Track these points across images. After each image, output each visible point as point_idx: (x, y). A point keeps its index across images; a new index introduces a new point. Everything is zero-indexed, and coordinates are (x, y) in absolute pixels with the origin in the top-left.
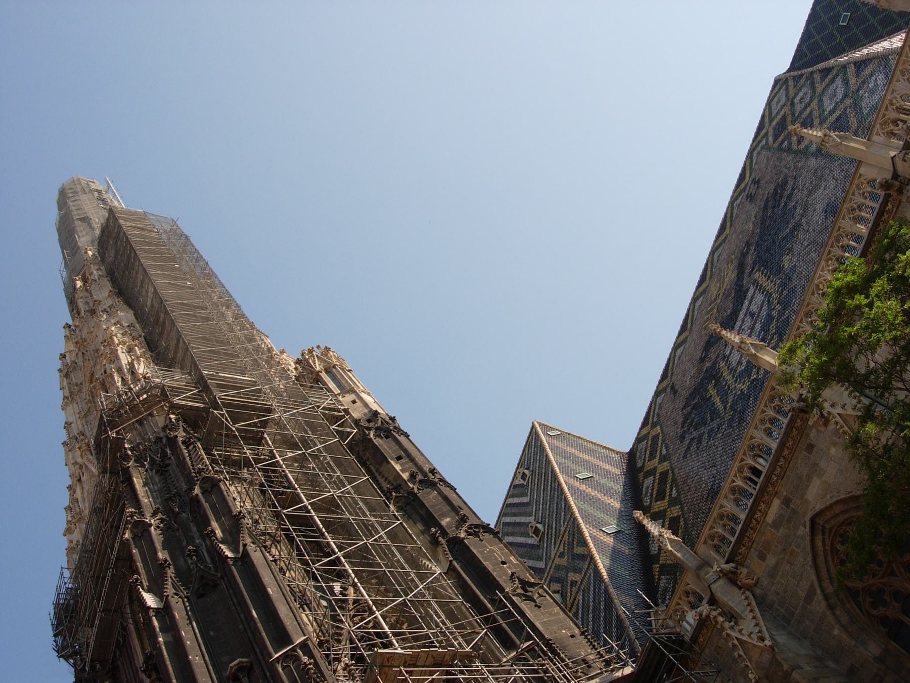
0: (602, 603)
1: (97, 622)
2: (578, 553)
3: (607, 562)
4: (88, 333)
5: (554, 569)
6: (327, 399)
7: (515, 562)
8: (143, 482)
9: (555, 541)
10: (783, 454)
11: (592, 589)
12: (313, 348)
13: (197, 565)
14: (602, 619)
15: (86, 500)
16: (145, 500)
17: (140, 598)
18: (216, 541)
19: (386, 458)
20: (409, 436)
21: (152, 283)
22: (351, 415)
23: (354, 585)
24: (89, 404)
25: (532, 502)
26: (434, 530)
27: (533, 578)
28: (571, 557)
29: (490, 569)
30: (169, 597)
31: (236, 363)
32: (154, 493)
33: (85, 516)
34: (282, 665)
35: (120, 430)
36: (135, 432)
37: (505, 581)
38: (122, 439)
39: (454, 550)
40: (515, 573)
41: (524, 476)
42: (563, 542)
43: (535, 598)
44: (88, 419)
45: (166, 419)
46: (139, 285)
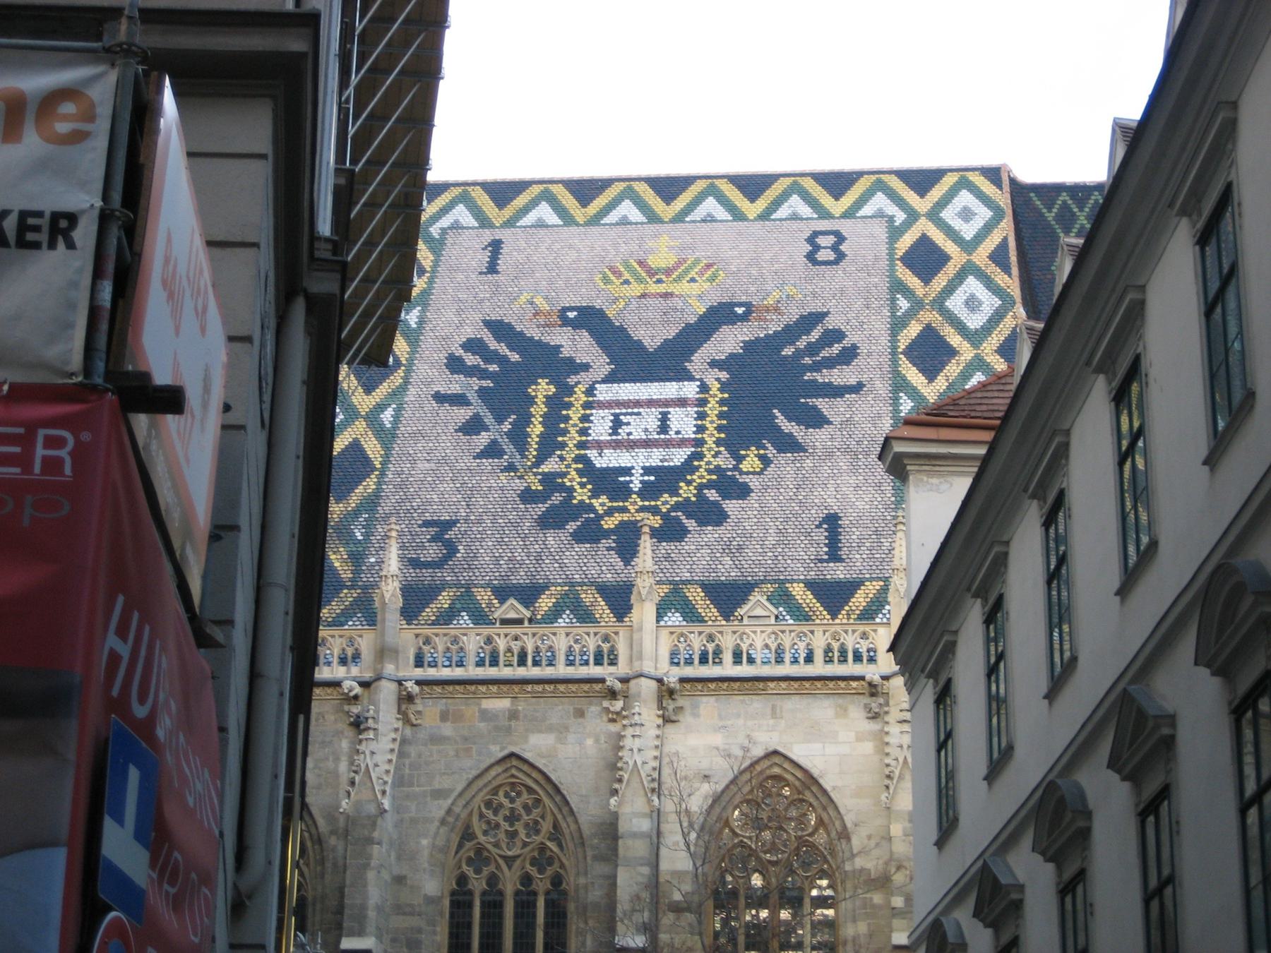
10: (558, 686)
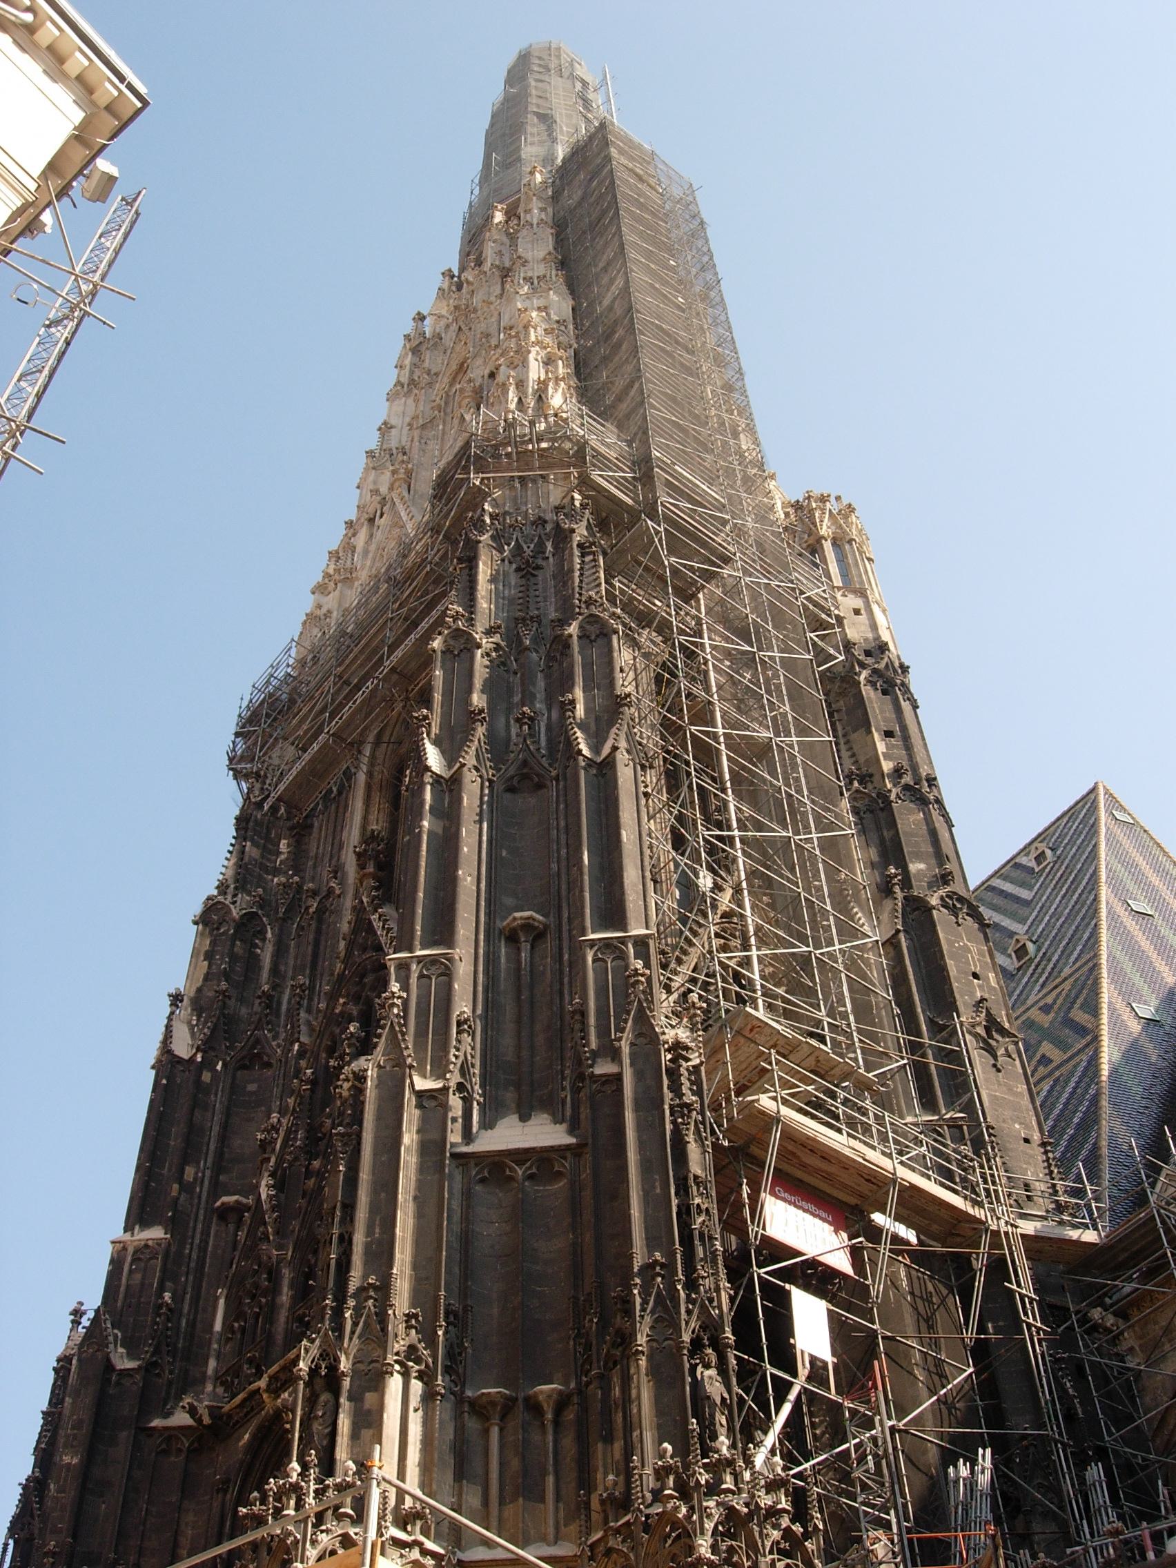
0: (1079, 1115)
1: (316, 747)
2: (1077, 1019)
3: (1117, 1056)
4: (484, 301)
5: (1023, 1023)
6: (819, 587)
7: (993, 983)
8: (491, 575)
9: (1044, 983)
11: (1072, 1084)
12: (829, 496)
13: (525, 740)
14: (1066, 1137)
15: (370, 555)
16: (483, 606)
17: (418, 747)
18: (571, 720)
19: (870, 723)
20: (918, 707)
21: (626, 273)
22: (844, 629)
23: (738, 890)
24: (436, 412)
25: (1034, 903)
26: (893, 871)
27: (1009, 1022)
28: (1059, 1019)
29: (951, 974)
30: (465, 769)
31: (705, 461)
32: (501, 601)
33: (357, 579)
34: (595, 955)
35: (488, 479)
36: (507, 492)
37: (965, 1003)
38: (486, 493)
39: (910, 917)
40: (986, 1000)
41: (1040, 858)
42: (1059, 990)
43: (999, 1054)
44: (425, 433)
45: (567, 494)
46: (601, 265)
